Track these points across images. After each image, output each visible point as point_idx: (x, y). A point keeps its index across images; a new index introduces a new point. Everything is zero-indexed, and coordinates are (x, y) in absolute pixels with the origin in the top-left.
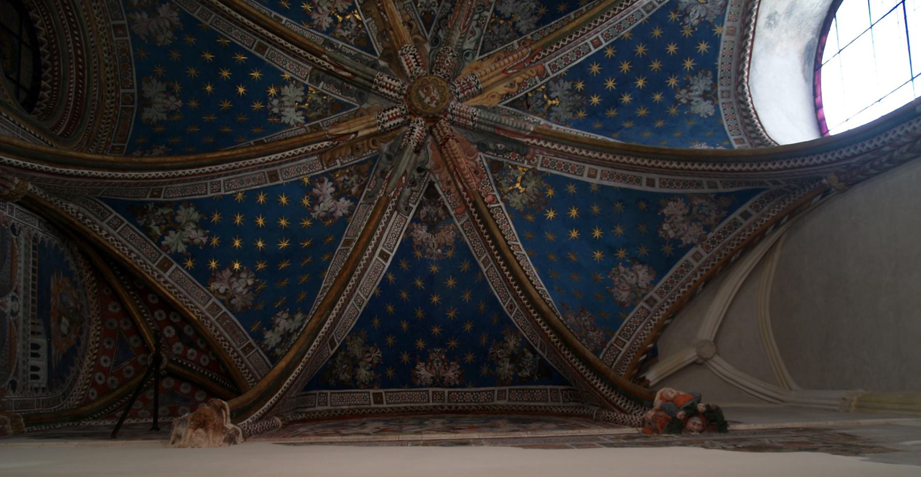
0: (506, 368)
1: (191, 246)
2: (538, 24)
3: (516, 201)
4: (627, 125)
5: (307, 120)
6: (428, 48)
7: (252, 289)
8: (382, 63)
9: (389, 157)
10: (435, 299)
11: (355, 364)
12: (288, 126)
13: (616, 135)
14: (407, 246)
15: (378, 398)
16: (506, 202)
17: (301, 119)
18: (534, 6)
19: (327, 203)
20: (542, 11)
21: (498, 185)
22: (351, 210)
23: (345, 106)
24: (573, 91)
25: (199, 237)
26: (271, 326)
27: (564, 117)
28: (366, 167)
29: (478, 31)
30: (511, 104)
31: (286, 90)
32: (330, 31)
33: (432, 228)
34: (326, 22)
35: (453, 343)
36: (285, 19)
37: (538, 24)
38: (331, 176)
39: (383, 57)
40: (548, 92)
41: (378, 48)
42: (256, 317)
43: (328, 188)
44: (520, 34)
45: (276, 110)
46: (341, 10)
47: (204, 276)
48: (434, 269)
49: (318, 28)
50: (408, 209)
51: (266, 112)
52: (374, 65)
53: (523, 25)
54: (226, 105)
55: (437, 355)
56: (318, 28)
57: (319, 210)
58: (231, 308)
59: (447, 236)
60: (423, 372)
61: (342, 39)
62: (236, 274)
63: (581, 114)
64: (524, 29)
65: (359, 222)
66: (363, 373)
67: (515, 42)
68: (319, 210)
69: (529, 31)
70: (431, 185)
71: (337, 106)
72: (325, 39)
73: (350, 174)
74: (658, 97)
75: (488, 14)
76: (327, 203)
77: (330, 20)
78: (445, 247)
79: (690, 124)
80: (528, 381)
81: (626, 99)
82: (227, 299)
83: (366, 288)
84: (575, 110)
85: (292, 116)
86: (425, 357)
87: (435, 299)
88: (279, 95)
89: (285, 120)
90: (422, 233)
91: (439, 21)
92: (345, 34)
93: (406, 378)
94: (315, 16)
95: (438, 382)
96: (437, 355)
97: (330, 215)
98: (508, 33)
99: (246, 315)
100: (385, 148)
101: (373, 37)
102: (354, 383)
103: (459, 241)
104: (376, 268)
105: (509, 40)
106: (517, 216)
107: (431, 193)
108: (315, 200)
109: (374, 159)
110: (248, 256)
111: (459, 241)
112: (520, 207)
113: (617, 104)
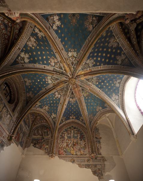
0: (81, 120)
1: (39, 105)
2: (93, 66)
3: (85, 95)
4: (104, 87)
5: (52, 82)
6: (72, 69)
7: (48, 108)
8: (64, 72)
9: (66, 88)
10: (73, 108)
11: (63, 120)
12: (49, 84)
13: (102, 89)
14: (69, 102)
15: (65, 122)
16: (83, 95)
17: (51, 82)
18: (93, 62)
19: (57, 96)
20: (94, 63)
21: (83, 92)
22: (61, 97)
23: (58, 79)
24: (97, 79)
25: (40, 104)
26: (52, 115)
27: (94, 83)
28: (62, 90)
29: (82, 66)
30: (86, 80)
31: (48, 77)
32: (54, 66)
33: (72, 98)
34: (53, 64)
35: (75, 114)
36: (46, 66)
37: (93, 66)
38: (57, 91)
39: (64, 70)
40: (93, 79)
41: (63, 69)
42: (50, 113)
43: (57, 93)
44: (90, 68)
45: (47, 80)
46: (56, 62)
47: (42, 108)
48: (73, 104)
49: (52, 66)
50: (69, 96)
51: (45, 81)
52: (62, 73)
53: (90, 65)
54: (39, 81)
55: (72, 115)
56: (52, 66)
57: (56, 97)
58: (46, 111)
59: (74, 99)
60: (71, 117)
61: (57, 67)
62: (46, 106)
63: (97, 83)
64: (90, 66)
65: (62, 100)
66: (64, 120)
67: (88, 69)
68: (56, 97)
69: (91, 67)
70: (72, 92)
71: (57, 79)
72: (54, 68)
73: (60, 91)
74: (111, 82)
75: (84, 64)
76: (57, 96)
77: (54, 64)
78: (74, 101)
79: (114, 88)
80: (83, 123)
81: (105, 81)
82: (45, 109)
83: (64, 110)
84: (96, 82)
85: (50, 82)
86: (71, 116)
87: (73, 108)
88: (47, 78)
89: (49, 82)
90: (71, 99)
91: (75, 64)
92: (57, 66)
93: (69, 119)
94: (51, 63)
95: (73, 118)
96: (72, 115)
97: (58, 97)
98: (87, 66)
99: (48, 112)
100: (65, 86)
101: (62, 67)
102: (63, 122)
103: (76, 100)
104: (65, 107)
105: (87, 68)
106: (85, 98)
107: (72, 93)
108: (55, 95)
109: (64, 88)
110: (47, 104)
111: (76, 100)
112: (86, 96)
113: (104, 82)
